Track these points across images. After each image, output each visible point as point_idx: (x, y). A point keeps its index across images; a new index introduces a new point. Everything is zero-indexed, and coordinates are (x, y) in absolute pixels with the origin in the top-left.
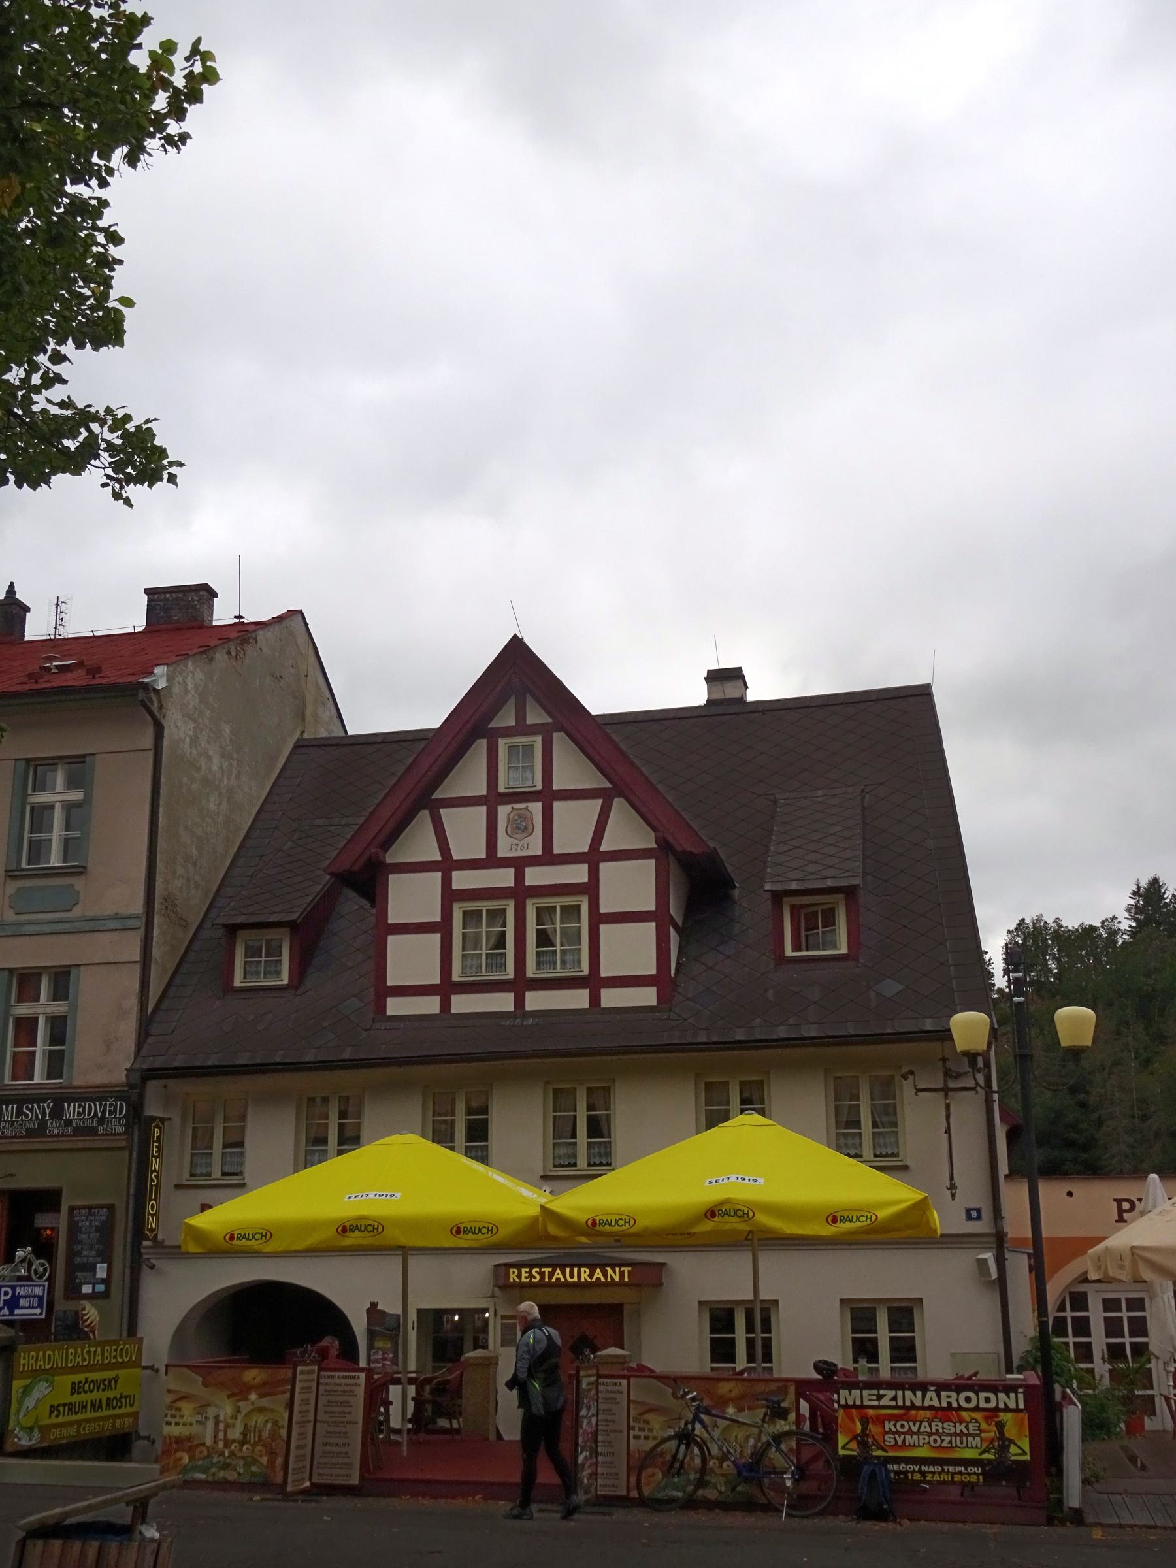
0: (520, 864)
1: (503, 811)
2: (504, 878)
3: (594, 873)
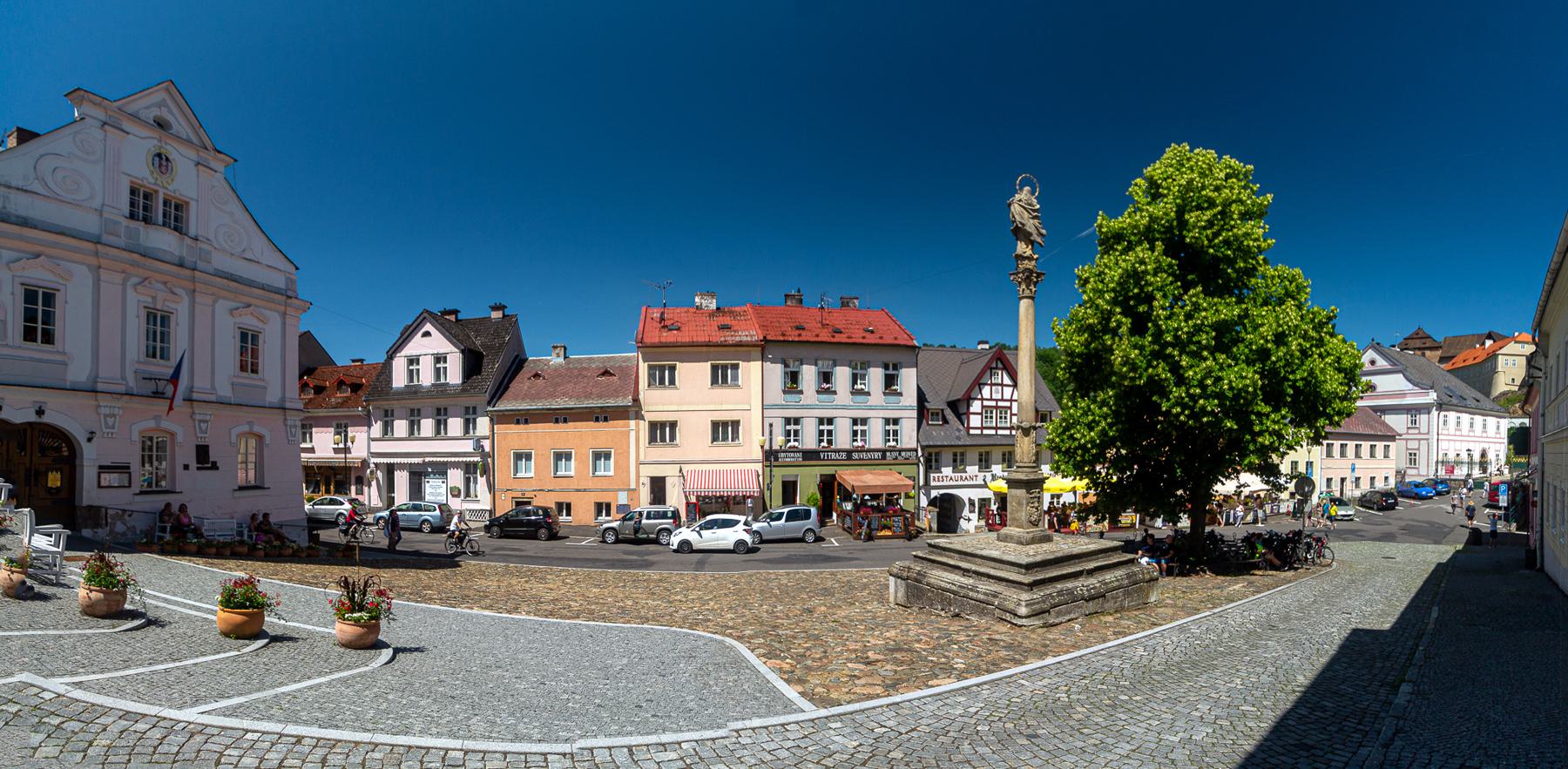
0: (997, 400)
1: (993, 388)
2: (993, 403)
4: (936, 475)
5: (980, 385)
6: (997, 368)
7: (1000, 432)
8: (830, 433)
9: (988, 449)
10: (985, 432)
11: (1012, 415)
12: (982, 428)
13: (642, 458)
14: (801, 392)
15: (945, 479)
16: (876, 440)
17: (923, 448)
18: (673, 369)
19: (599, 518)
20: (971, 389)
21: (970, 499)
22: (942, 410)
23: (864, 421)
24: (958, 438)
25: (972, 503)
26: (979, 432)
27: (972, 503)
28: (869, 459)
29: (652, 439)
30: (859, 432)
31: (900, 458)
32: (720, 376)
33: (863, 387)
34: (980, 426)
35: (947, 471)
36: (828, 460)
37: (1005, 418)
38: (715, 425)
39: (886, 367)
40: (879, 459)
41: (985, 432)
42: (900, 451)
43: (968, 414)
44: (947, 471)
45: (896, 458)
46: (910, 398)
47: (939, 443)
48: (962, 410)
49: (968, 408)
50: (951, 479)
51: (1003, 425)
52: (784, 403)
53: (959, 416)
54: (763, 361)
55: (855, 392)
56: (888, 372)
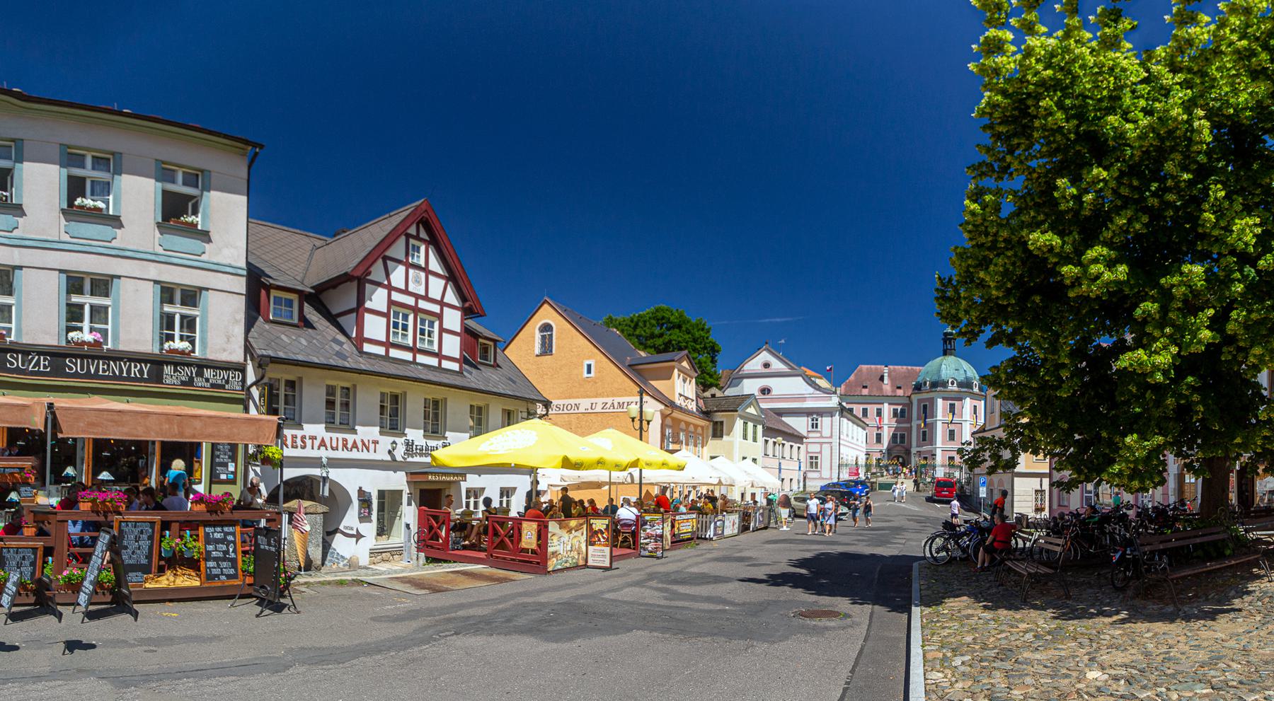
0: (417, 297)
2: (410, 301)
3: (442, 310)
5: (385, 259)
10: (394, 353)
11: (442, 330)
12: (388, 345)
15: (309, 442)
17: (263, 363)
20: (369, 261)
21: (361, 491)
23: (102, 285)
25: (365, 500)
26: (381, 351)
27: (365, 500)
28: (114, 377)
30: (87, 309)
31: (199, 382)
40: (141, 380)
41: (394, 353)
42: (202, 365)
43: (359, 309)
44: (316, 430)
45: (190, 382)
50: (323, 443)
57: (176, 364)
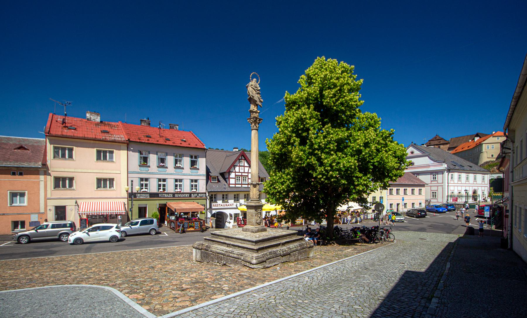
0: (242, 173)
2: (240, 174)
4: (215, 204)
6: (242, 159)
7: (243, 186)
8: (164, 185)
9: (238, 193)
10: (237, 186)
11: (248, 179)
12: (235, 184)
13: (49, 196)
14: (149, 167)
16: (186, 188)
18: (71, 150)
19: (16, 230)
20: (230, 168)
22: (218, 177)
24: (225, 188)
29: (57, 186)
31: (198, 196)
32: (101, 156)
33: (180, 165)
34: (234, 183)
35: (220, 202)
36: (163, 197)
37: (246, 180)
38: (99, 180)
39: (191, 157)
41: (237, 186)
42: (198, 194)
43: (229, 178)
46: (203, 171)
47: (216, 190)
48: (227, 176)
49: (229, 176)
50: (222, 205)
51: (245, 183)
52: (139, 171)
53: (225, 179)
54: (128, 150)
55: (176, 168)
56: (192, 159)
57: (194, 194)
